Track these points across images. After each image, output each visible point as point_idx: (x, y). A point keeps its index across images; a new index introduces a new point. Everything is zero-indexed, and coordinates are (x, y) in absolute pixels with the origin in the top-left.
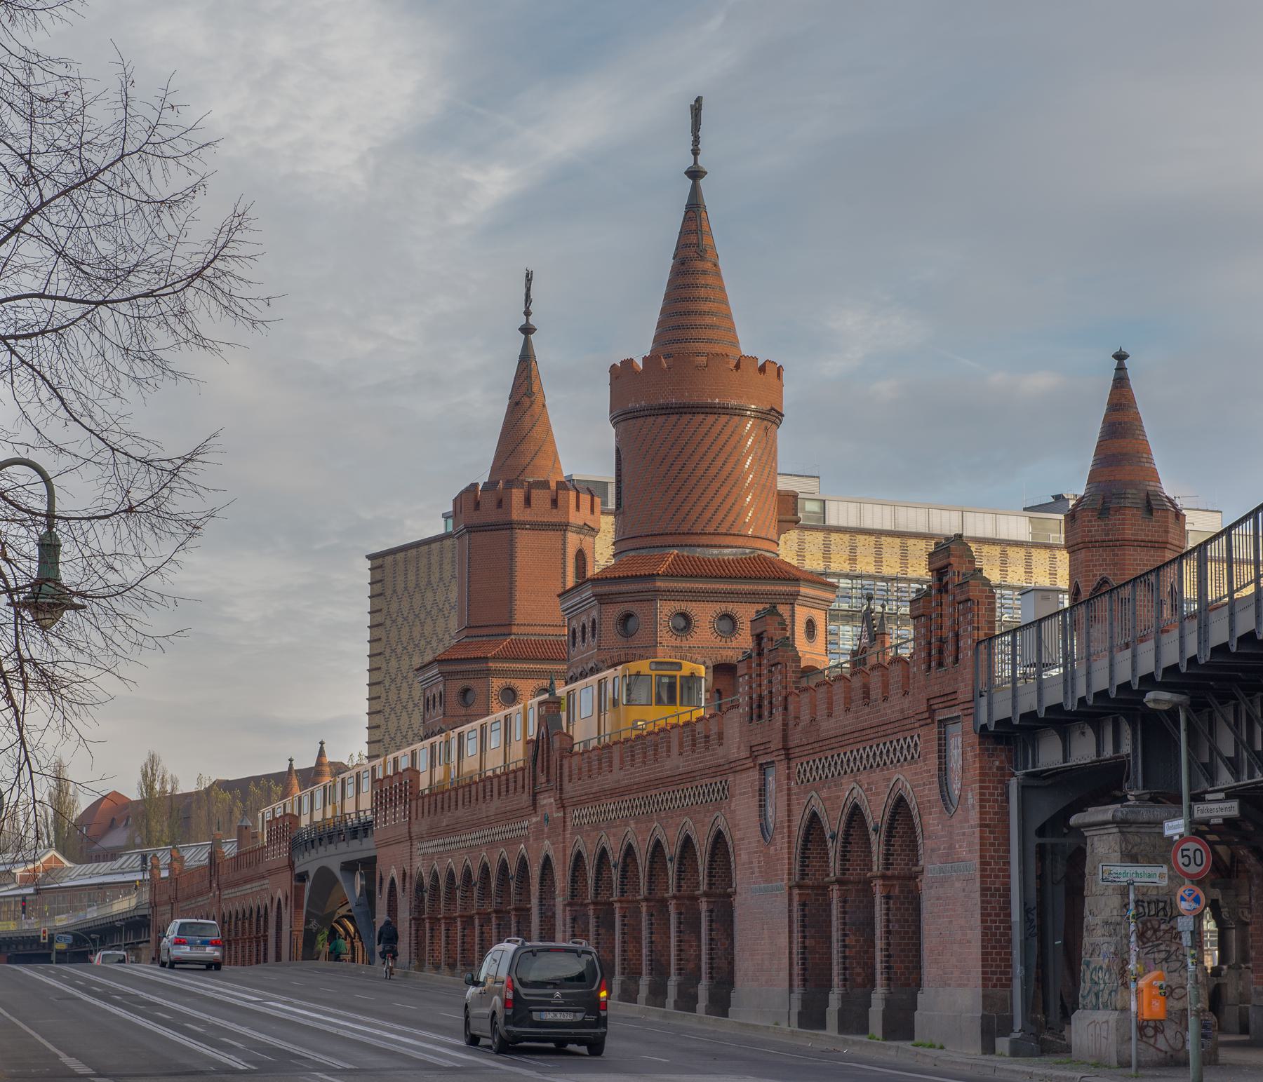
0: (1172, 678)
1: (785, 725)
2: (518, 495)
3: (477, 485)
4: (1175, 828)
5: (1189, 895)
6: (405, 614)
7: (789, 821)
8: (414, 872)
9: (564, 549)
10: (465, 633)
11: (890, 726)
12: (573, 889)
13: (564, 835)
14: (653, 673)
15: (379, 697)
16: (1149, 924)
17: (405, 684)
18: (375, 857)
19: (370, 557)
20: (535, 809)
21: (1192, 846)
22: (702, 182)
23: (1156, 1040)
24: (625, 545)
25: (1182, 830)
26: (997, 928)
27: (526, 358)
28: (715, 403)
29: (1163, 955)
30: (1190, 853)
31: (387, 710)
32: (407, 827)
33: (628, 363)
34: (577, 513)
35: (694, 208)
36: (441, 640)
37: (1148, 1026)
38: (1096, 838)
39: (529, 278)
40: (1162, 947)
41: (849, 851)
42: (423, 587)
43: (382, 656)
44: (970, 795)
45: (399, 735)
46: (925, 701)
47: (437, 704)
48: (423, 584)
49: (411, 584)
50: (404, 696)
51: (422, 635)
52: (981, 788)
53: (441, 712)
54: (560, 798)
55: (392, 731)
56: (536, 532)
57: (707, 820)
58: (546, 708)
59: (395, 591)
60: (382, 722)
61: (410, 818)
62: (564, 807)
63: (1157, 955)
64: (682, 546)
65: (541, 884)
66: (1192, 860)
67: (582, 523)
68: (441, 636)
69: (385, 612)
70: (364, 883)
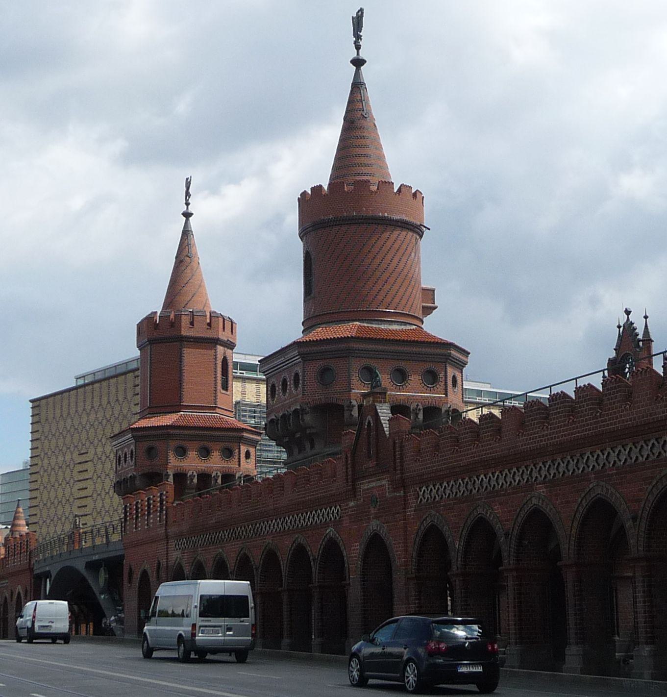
3: (156, 313)
15: (37, 481)
17: (53, 473)
18: (122, 557)
19: (31, 401)
24: (309, 324)
28: (385, 216)
34: (224, 333)
35: (357, 85)
43: (39, 457)
45: (49, 502)
47: (129, 459)
49: (58, 415)
50: (53, 480)
55: (45, 500)
60: (38, 495)
67: (226, 340)
70: (107, 576)
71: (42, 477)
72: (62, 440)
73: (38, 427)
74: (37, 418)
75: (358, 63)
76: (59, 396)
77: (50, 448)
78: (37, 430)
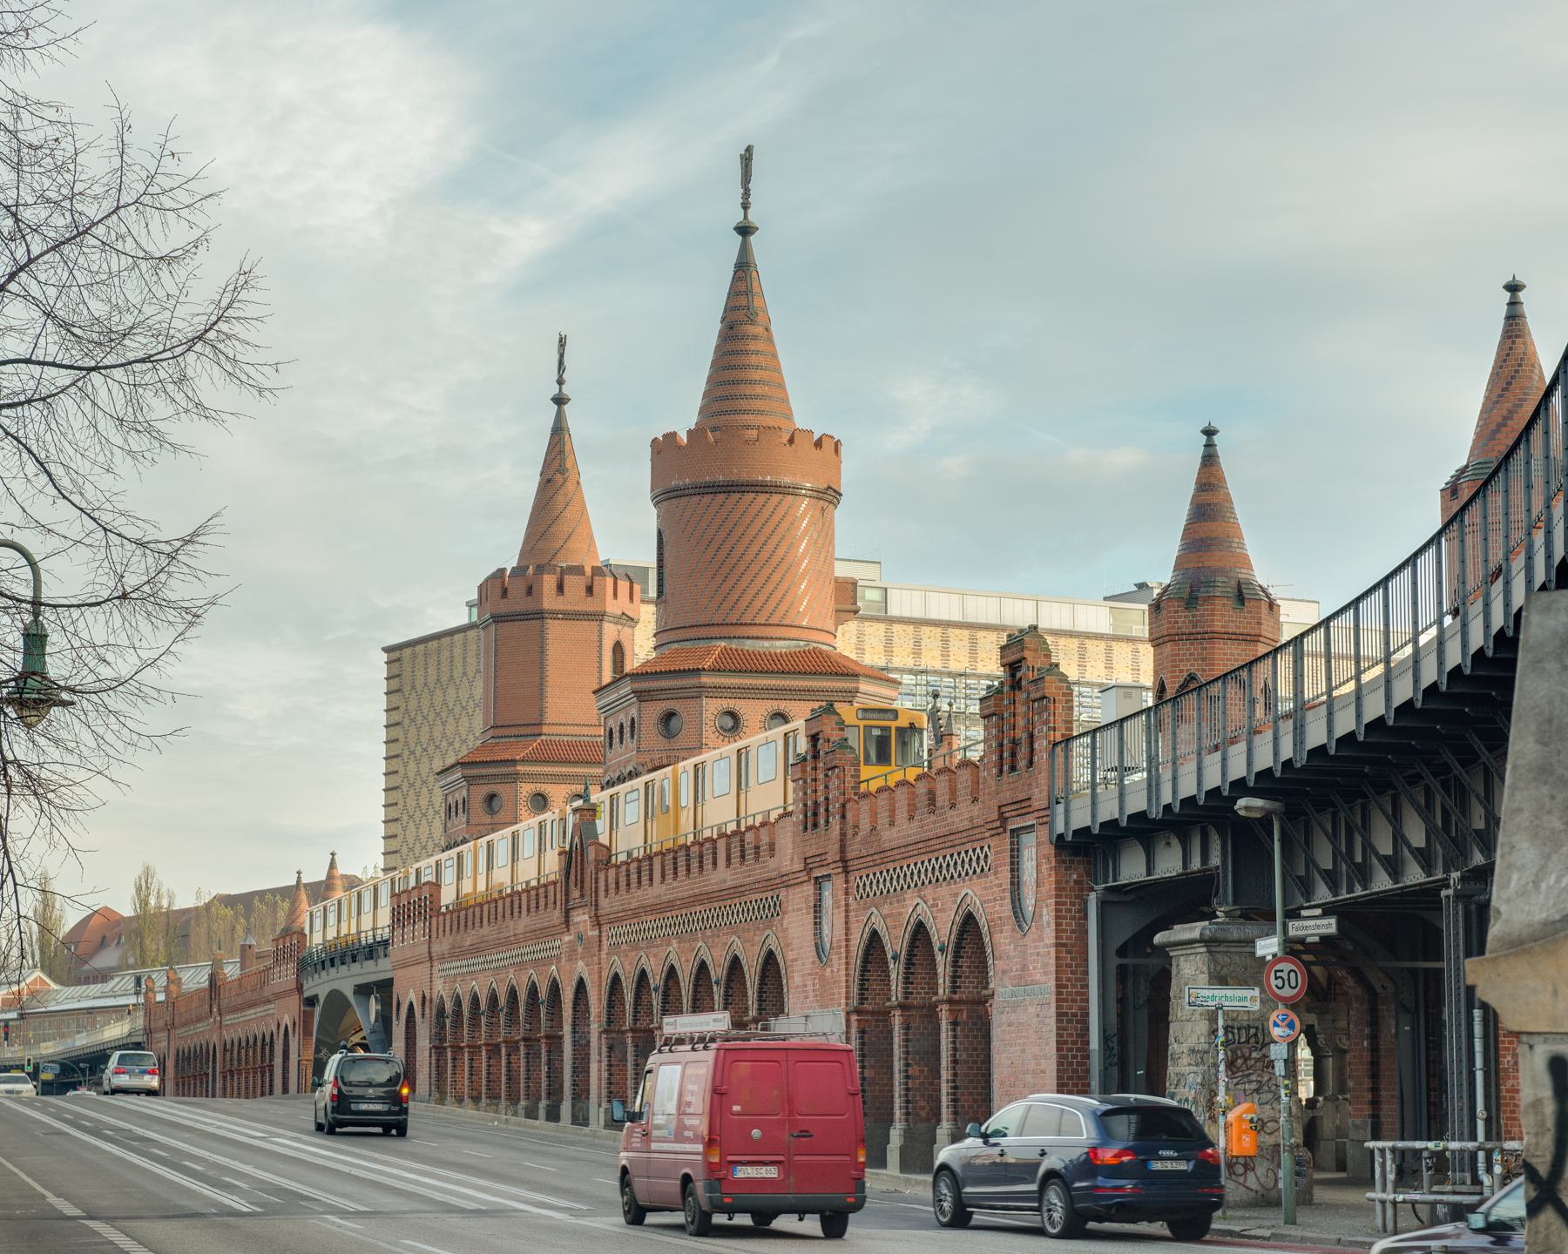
0: (1264, 783)
1: (843, 834)
2: (549, 582)
4: (1268, 947)
5: (1283, 1020)
6: (425, 712)
7: (847, 940)
8: (434, 996)
9: (600, 641)
10: (491, 733)
11: (957, 836)
12: (609, 1014)
13: (599, 955)
14: (862, 723)
15: (396, 804)
16: (1239, 1052)
17: (424, 790)
19: (387, 650)
20: (568, 927)
21: (1286, 966)
22: (753, 239)
23: (1246, 1178)
24: (666, 637)
25: (1275, 949)
26: (1074, 1057)
27: (559, 431)
29: (1254, 1086)
30: (1284, 975)
31: (405, 817)
32: (427, 946)
33: (671, 437)
35: (744, 267)
36: (465, 741)
37: (1236, 1163)
38: (1182, 959)
39: (562, 343)
40: (1254, 1077)
41: (913, 973)
42: (444, 683)
43: (400, 759)
44: (1045, 912)
45: (418, 845)
46: (996, 808)
47: (460, 811)
48: (444, 679)
49: (432, 680)
50: (424, 803)
51: (444, 735)
52: (1057, 903)
53: (464, 820)
54: (596, 914)
55: (411, 840)
56: (570, 622)
57: (757, 938)
58: (581, 815)
59: (413, 687)
60: (399, 831)
61: (430, 937)
62: (599, 925)
63: (1247, 1086)
64: (730, 638)
65: (574, 1009)
66: (1286, 982)
68: (464, 737)
69: (402, 709)
70: (379, 1007)
71: (405, 797)
72: (440, 728)
73: (397, 700)
74: (395, 684)
75: (745, 230)
76: (435, 643)
77: (418, 742)
78: (396, 706)
